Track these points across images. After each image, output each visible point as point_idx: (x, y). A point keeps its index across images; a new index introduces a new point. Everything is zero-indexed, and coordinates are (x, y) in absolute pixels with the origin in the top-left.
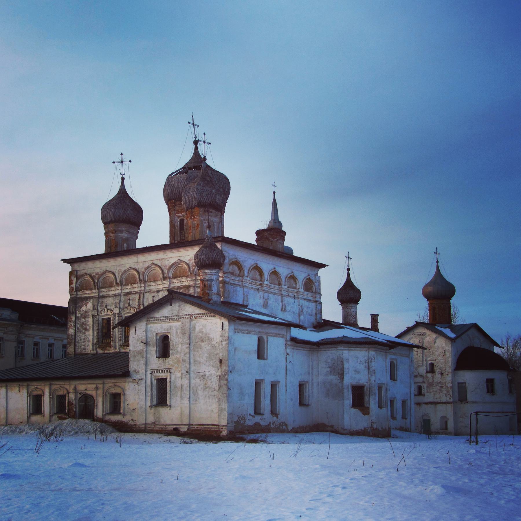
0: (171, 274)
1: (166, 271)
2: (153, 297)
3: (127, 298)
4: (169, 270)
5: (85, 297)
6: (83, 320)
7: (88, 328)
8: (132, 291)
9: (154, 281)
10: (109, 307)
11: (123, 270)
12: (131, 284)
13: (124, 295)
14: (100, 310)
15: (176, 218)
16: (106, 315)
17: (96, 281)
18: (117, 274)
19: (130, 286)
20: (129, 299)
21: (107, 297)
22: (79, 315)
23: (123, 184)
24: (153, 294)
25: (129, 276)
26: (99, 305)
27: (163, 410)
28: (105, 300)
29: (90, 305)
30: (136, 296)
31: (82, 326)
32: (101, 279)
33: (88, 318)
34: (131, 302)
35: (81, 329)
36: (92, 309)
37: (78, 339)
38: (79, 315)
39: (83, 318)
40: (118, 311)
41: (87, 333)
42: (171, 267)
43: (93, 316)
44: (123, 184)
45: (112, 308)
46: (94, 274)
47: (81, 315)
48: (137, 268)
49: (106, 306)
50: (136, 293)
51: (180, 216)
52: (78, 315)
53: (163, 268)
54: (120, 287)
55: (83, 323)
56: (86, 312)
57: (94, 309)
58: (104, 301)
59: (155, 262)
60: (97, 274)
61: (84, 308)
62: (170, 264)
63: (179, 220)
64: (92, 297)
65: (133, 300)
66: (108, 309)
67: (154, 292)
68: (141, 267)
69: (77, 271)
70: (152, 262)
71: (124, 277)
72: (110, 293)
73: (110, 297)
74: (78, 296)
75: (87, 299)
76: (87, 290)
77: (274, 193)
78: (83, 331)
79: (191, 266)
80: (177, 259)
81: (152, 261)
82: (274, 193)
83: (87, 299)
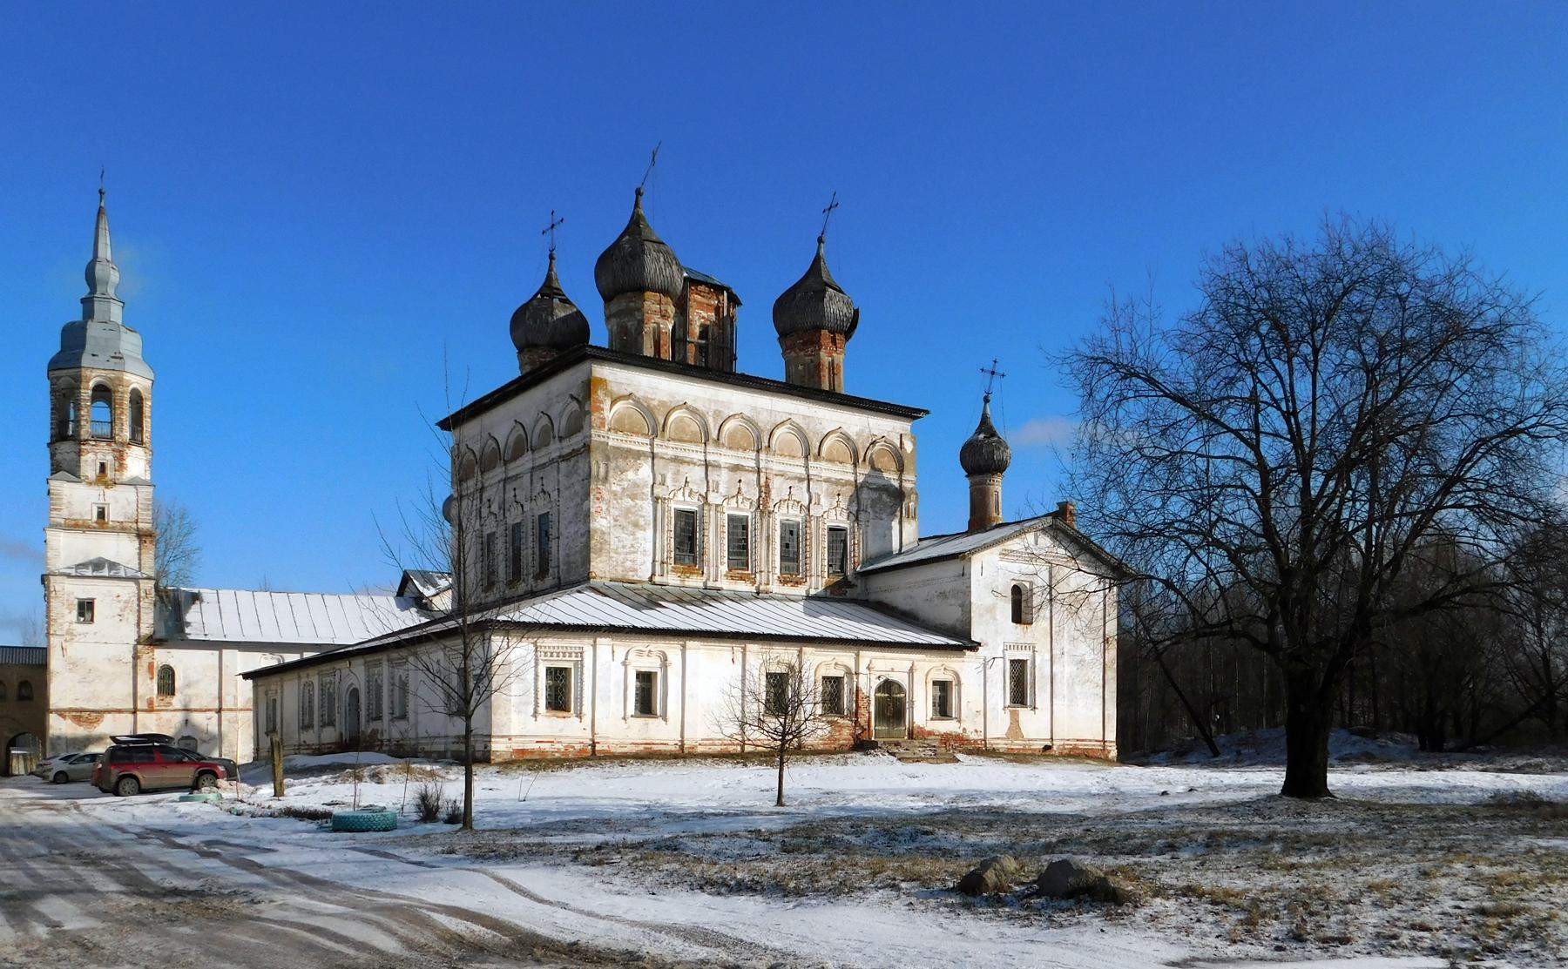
3: (738, 475)
5: (629, 451)
6: (628, 502)
7: (642, 522)
10: (695, 489)
19: (740, 454)
24: (791, 483)
27: (1024, 713)
28: (684, 469)
29: (645, 471)
31: (626, 517)
35: (622, 521)
37: (614, 543)
41: (639, 534)
55: (628, 511)
56: (636, 485)
61: (630, 475)
68: (764, 421)
75: (638, 455)
78: (630, 528)
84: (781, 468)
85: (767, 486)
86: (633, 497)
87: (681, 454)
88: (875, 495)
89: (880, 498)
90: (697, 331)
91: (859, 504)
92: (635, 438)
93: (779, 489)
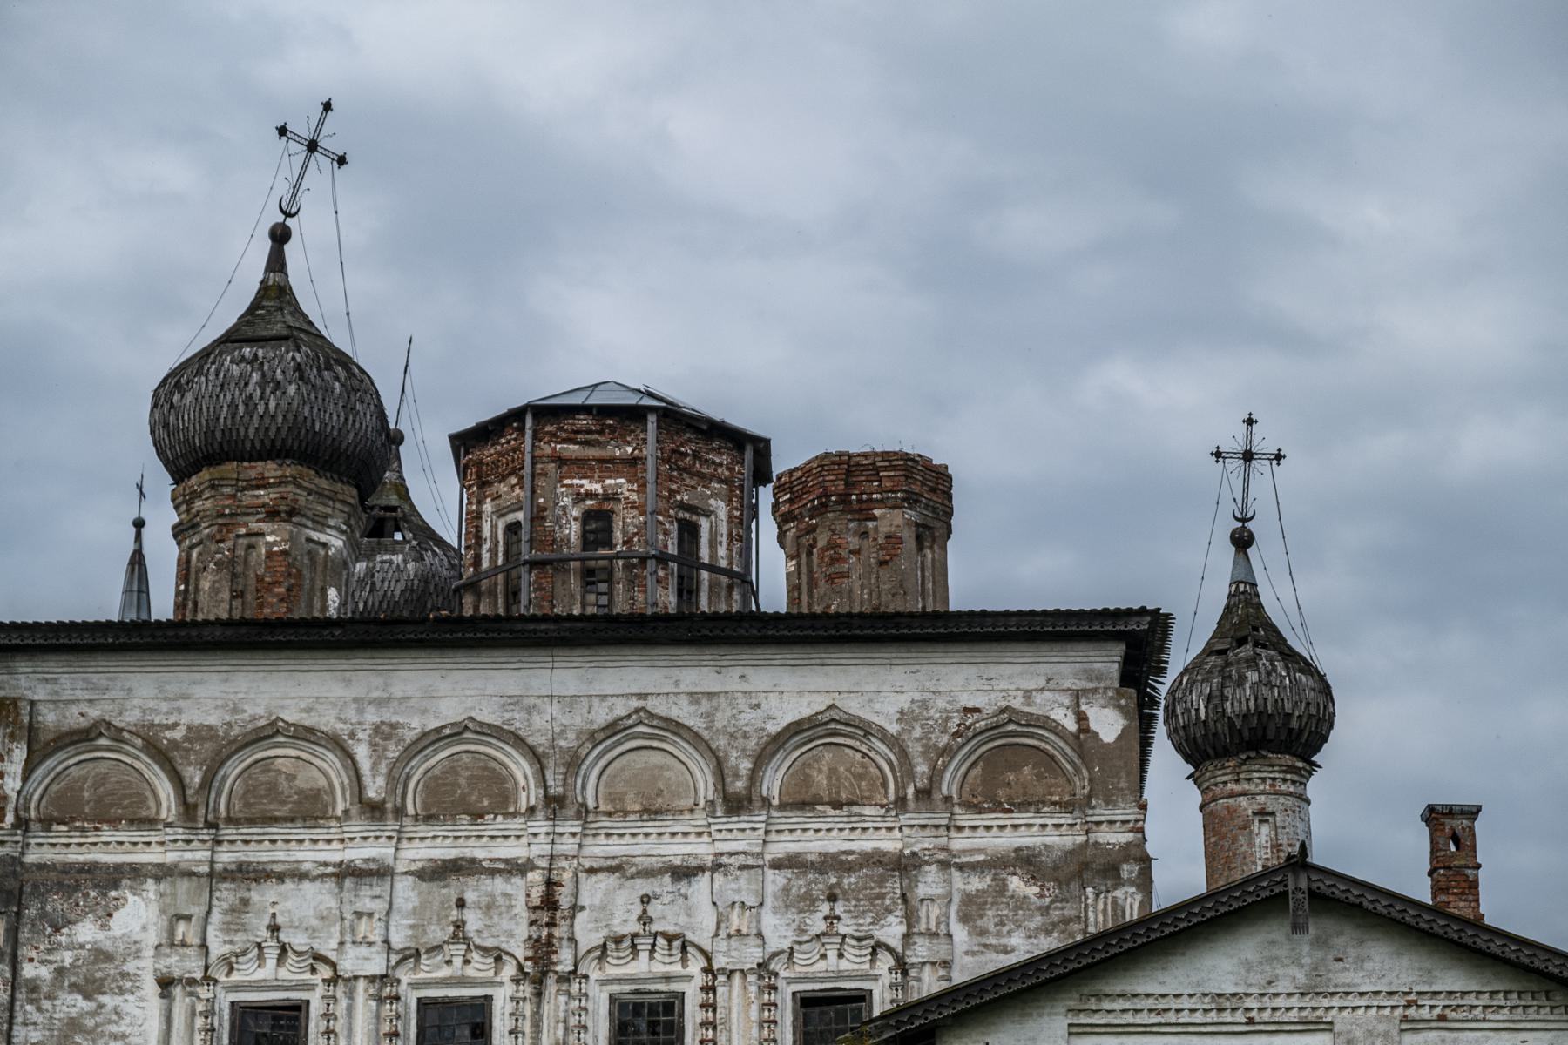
0: (773, 783)
1: (745, 765)
2: (646, 900)
4: (761, 760)
5: (90, 869)
6: (73, 1004)
8: (480, 854)
9: (651, 812)
10: (298, 940)
11: (416, 724)
12: (477, 816)
13: (421, 875)
14: (217, 948)
15: (567, 501)
16: (264, 979)
17: (194, 776)
18: (362, 752)
19: (465, 826)
20: (461, 904)
21: (281, 877)
22: (45, 972)
23: (277, 262)
25: (453, 771)
26: (216, 917)
28: (264, 895)
29: (137, 916)
30: (522, 892)
32: (233, 769)
33: (122, 991)
34: (473, 921)
36: (152, 938)
38: (45, 972)
39: (75, 987)
40: (377, 966)
42: (778, 742)
43: (166, 984)
44: (277, 262)
45: (328, 947)
46: (178, 735)
47: (60, 972)
48: (518, 721)
49: (274, 928)
50: (517, 868)
51: (590, 495)
52: (28, 971)
53: (721, 742)
54: (391, 826)
56: (101, 955)
57: (173, 943)
58: (255, 896)
59: (659, 707)
60: (198, 733)
61: (86, 932)
62: (773, 728)
63: (576, 512)
64: (163, 873)
65: (489, 908)
66: (283, 950)
67: (648, 873)
69: (32, 703)
70: (636, 703)
71: (418, 771)
72: (307, 856)
73: (302, 876)
74: (31, 858)
75: (112, 878)
76: (114, 823)
77: (139, 524)
79: (914, 749)
80: (819, 704)
81: (642, 696)
82: (139, 524)
83: (112, 878)
84: (616, 848)
85: (549, 902)
86: (90, 988)
87: (259, 855)
88: (976, 883)
89: (1001, 888)
90: (573, 530)
91: (910, 918)
92: (107, 835)
93: (603, 907)
